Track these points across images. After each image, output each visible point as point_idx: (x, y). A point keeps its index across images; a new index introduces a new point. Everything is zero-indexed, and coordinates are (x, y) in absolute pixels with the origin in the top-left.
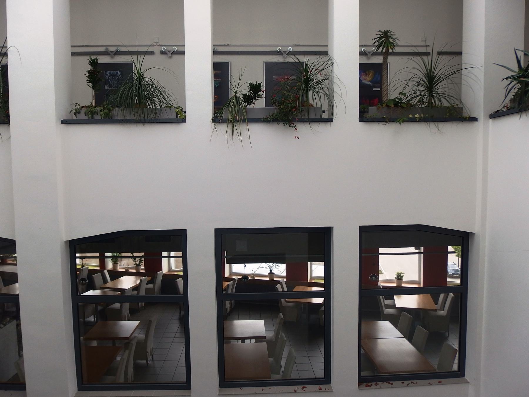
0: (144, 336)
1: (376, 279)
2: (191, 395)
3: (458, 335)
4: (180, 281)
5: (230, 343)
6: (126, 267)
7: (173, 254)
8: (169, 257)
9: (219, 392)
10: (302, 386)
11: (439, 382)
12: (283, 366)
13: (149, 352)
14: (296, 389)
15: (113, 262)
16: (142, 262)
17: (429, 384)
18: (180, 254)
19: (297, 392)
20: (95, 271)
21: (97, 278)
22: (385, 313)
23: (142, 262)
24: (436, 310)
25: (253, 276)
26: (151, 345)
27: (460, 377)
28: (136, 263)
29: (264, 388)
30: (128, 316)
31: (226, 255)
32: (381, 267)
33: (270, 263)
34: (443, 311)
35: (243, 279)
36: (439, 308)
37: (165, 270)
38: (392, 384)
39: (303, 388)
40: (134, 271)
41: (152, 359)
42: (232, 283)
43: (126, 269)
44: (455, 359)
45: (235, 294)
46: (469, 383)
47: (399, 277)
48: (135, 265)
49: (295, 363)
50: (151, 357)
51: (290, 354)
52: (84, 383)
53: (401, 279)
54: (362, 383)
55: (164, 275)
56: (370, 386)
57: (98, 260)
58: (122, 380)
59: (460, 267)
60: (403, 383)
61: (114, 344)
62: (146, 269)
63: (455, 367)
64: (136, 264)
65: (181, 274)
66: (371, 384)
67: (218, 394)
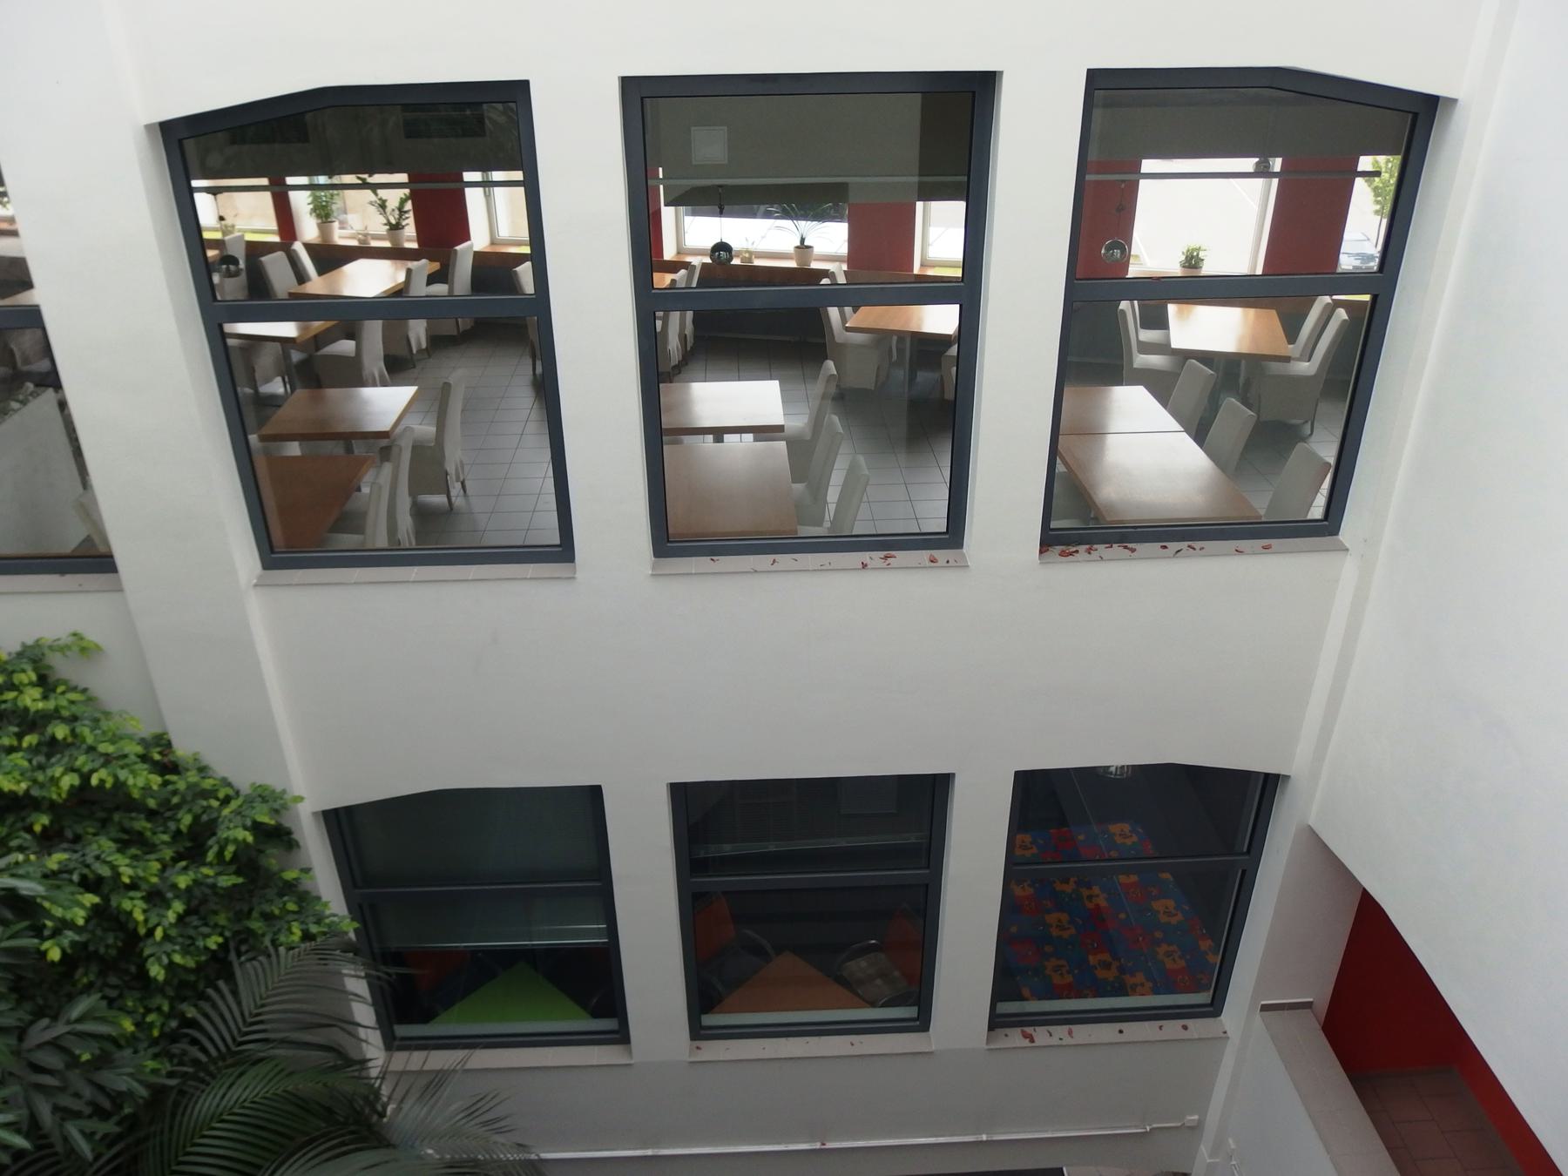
0: (433, 429)
1: (1121, 256)
2: (576, 576)
3: (1339, 432)
4: (525, 271)
5: (679, 442)
6: (359, 234)
7: (497, 176)
8: (487, 184)
9: (653, 568)
10: (882, 554)
11: (1264, 548)
12: (832, 508)
13: (454, 472)
14: (867, 561)
15: (319, 216)
16: (407, 218)
17: (1237, 551)
18: (518, 175)
19: (869, 567)
20: (268, 248)
21: (276, 266)
22: (1135, 366)
23: (407, 215)
24: (1287, 359)
25: (747, 255)
26: (454, 455)
27: (1324, 536)
28: (388, 220)
29: (778, 557)
30: (382, 376)
31: (661, 176)
32: (1139, 243)
33: (797, 220)
34: (1307, 364)
35: (717, 254)
36: (1297, 355)
37: (479, 240)
38: (1133, 550)
39: (886, 557)
40: (387, 244)
41: (462, 491)
42: (684, 276)
43: (359, 240)
44: (1319, 494)
45: (695, 290)
46: (1347, 550)
47: (1192, 261)
48: (388, 227)
49: (865, 499)
50: (458, 485)
51: (852, 471)
52: (277, 550)
53: (1196, 268)
54: (1049, 546)
55: (478, 255)
56: (1071, 554)
57: (267, 197)
58: (382, 541)
59: (1380, 247)
60: (1165, 547)
61: (349, 450)
62: (421, 237)
63: (1317, 511)
64: (389, 223)
65: (526, 250)
66: (1074, 549)
67: (650, 572)
